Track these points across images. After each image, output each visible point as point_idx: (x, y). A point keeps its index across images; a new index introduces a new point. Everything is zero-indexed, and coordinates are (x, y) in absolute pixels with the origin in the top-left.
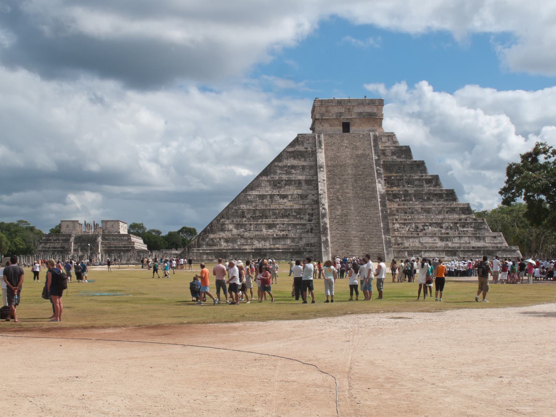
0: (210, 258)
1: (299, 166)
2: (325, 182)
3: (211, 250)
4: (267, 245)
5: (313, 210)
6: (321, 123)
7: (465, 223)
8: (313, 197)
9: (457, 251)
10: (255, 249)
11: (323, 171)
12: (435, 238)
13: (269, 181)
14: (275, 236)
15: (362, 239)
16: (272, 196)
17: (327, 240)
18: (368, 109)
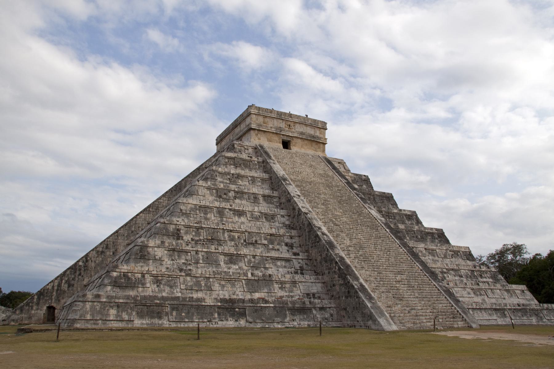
0: (125, 316)
1: (247, 177)
2: (303, 198)
3: (128, 297)
4: (240, 293)
5: (291, 238)
6: (257, 135)
7: (481, 271)
8: (283, 220)
9: (505, 309)
10: (223, 300)
11: (290, 184)
12: (467, 289)
13: (209, 188)
14: (249, 275)
15: (410, 286)
16: (221, 212)
17: (361, 285)
18: (310, 131)
